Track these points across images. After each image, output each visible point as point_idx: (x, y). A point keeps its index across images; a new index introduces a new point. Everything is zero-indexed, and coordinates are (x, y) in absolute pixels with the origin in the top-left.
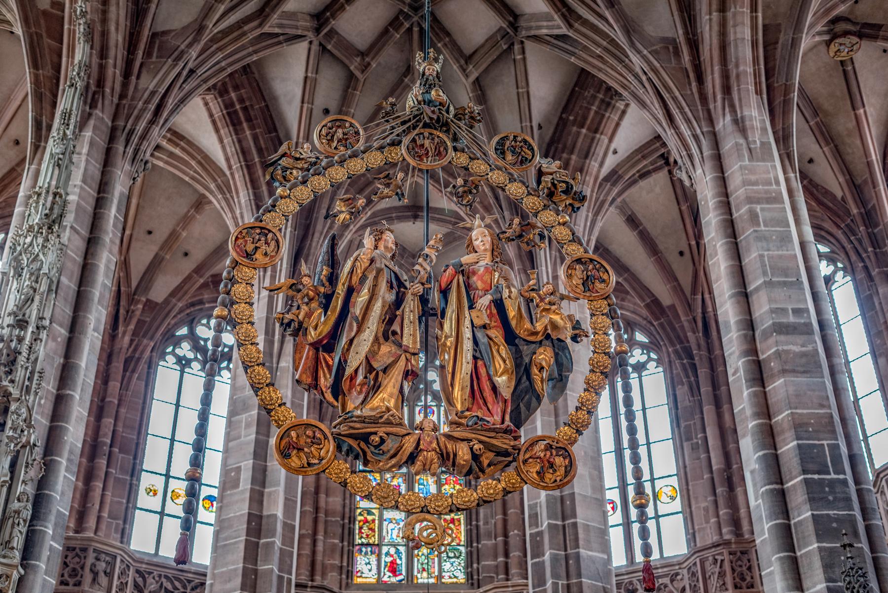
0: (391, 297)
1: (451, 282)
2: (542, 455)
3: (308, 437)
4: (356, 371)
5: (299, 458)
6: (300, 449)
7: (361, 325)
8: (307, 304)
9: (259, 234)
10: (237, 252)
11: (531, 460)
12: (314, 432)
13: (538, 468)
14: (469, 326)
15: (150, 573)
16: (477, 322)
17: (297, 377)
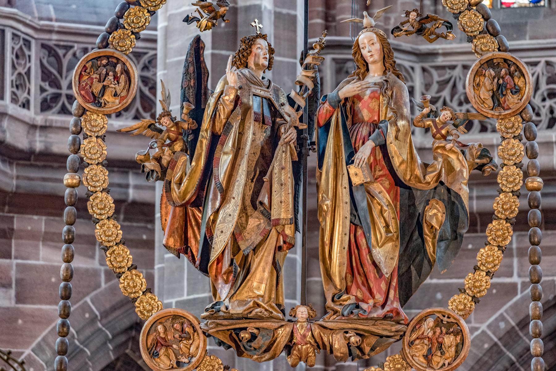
0: (262, 136)
1: (331, 116)
2: (430, 335)
3: (176, 330)
4: (223, 252)
5: (168, 356)
6: (168, 346)
7: (225, 193)
8: (169, 146)
9: (104, 66)
10: (83, 97)
11: (417, 342)
13: (425, 351)
14: (347, 186)
15: (68, 48)
16: (356, 181)
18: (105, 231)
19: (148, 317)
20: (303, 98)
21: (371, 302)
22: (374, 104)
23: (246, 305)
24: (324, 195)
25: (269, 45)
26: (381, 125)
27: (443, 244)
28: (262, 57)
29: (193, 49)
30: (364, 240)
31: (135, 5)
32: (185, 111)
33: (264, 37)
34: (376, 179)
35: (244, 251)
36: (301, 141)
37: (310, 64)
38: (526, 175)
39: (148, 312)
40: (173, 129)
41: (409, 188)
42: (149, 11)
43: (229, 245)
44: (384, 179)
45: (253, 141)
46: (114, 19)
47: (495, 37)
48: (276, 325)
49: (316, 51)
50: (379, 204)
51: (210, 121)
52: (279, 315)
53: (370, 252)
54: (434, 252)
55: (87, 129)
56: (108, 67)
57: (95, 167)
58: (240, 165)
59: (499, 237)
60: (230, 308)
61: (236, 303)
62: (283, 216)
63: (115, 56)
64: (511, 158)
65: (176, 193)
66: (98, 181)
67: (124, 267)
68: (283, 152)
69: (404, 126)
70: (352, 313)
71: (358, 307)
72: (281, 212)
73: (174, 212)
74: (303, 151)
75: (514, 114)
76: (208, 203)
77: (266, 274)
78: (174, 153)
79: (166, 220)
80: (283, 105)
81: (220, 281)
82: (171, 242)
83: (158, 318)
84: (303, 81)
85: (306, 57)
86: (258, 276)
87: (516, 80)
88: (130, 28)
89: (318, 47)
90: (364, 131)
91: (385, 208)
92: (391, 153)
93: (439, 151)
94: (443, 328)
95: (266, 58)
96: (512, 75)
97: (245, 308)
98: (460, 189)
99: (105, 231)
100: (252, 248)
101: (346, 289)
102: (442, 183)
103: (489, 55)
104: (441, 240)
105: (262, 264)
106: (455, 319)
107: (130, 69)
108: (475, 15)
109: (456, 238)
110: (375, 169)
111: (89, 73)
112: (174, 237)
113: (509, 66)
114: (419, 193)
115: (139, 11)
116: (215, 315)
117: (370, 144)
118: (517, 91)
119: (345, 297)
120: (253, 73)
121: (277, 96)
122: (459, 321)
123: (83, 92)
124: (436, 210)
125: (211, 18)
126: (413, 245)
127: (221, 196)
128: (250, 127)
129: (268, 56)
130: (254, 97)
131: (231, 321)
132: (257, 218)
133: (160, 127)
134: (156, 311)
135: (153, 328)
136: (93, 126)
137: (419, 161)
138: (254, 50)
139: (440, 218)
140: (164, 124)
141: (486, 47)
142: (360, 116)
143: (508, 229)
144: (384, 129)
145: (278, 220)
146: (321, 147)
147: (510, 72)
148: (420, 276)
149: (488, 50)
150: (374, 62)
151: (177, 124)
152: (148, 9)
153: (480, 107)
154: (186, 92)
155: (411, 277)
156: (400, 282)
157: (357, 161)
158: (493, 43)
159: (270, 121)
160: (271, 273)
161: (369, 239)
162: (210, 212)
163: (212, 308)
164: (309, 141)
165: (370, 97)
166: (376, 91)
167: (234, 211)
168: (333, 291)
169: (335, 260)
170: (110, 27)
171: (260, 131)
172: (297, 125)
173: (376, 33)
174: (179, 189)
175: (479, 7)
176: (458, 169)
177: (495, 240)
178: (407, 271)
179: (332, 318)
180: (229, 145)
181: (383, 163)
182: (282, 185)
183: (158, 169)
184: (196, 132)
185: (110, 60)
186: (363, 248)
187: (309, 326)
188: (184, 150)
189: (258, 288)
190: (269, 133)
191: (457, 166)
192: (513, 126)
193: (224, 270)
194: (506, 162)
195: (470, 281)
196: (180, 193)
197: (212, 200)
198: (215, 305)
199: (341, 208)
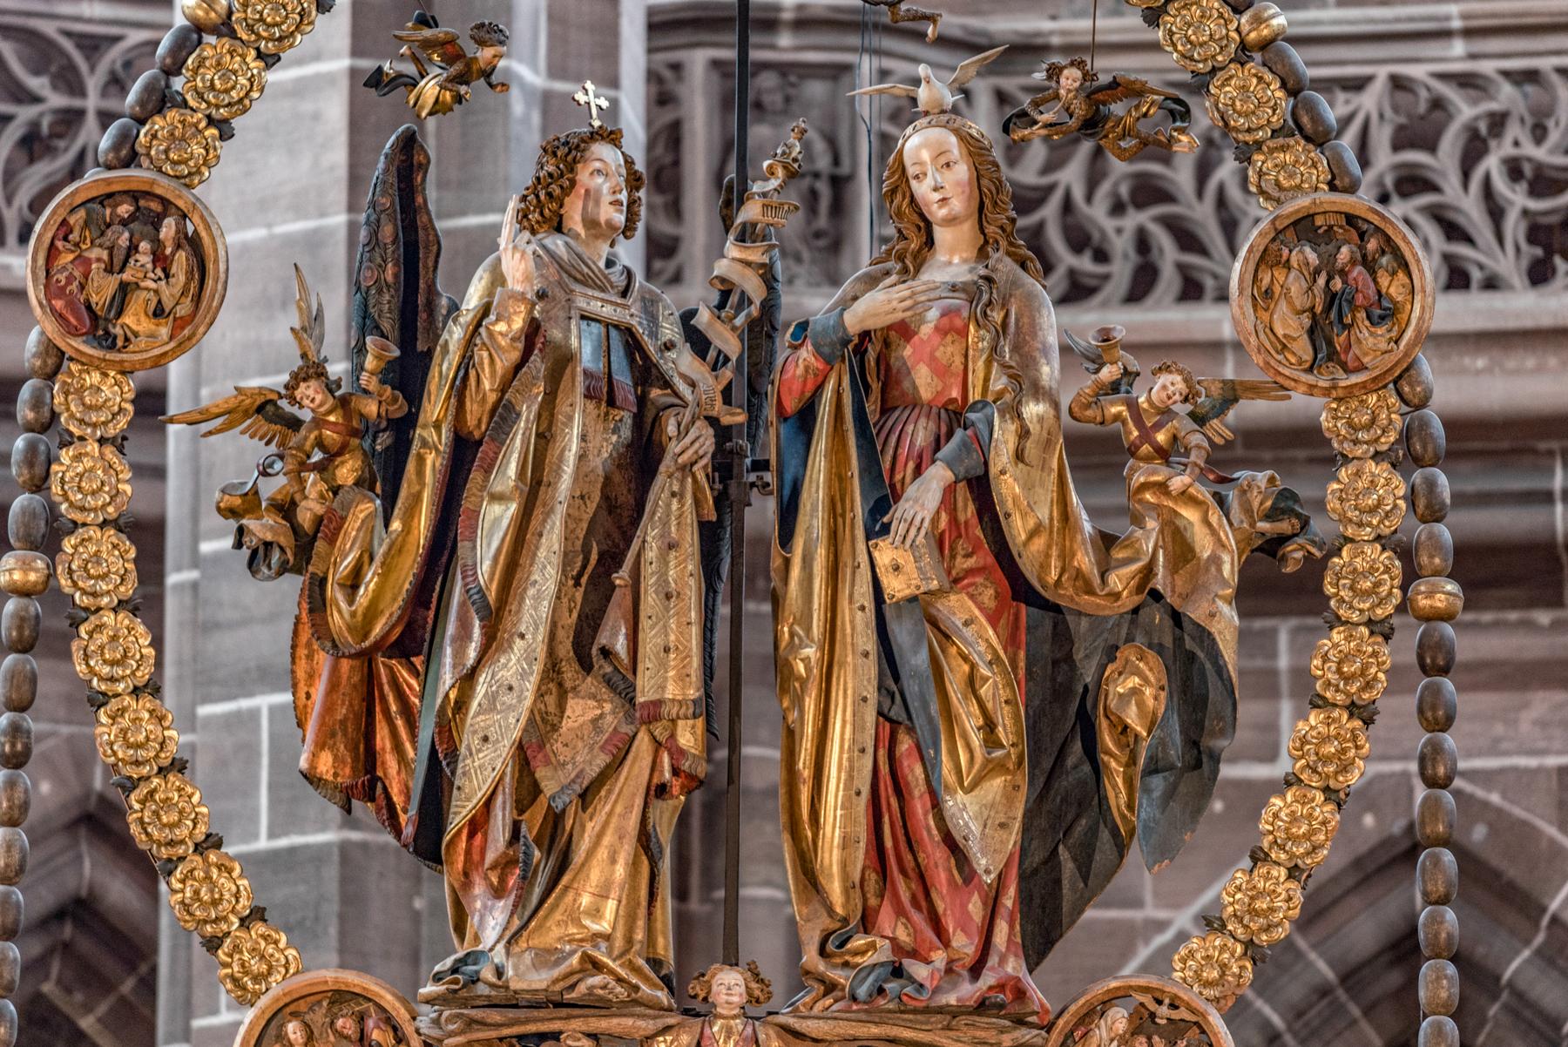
0: (608, 444)
1: (820, 388)
4: (489, 803)
7: (495, 620)
8: (321, 468)
9: (124, 223)
10: (60, 317)
12: (361, 1018)
16: (896, 587)
17: (303, 763)
18: (124, 731)
19: (257, 995)
20: (734, 329)
21: (939, 958)
22: (949, 352)
23: (557, 963)
24: (797, 628)
25: (629, 162)
26: (972, 416)
27: (1158, 783)
28: (607, 198)
29: (393, 169)
30: (918, 770)
31: (220, 35)
32: (370, 362)
33: (612, 137)
34: (956, 581)
35: (553, 797)
36: (724, 465)
37: (754, 225)
38: (1411, 575)
39: (256, 979)
40: (332, 418)
41: (1056, 609)
42: (260, 55)
43: (507, 779)
44: (979, 580)
45: (582, 457)
46: (154, 79)
47: (1320, 145)
48: (646, 1026)
49: (774, 183)
50: (965, 658)
51: (448, 398)
52: (659, 994)
53: (936, 805)
54: (1130, 807)
55: (72, 416)
56: (134, 226)
57: (93, 532)
58: (541, 535)
59: (1326, 760)
60: (510, 972)
61: (528, 958)
62: (672, 691)
63: (158, 191)
64: (1366, 518)
65: (340, 616)
66: (104, 577)
67: (182, 842)
68: (673, 494)
69: (1041, 419)
70: (881, 991)
71: (898, 972)
72: (666, 679)
73: (335, 670)
74: (733, 490)
75: (1377, 384)
76: (441, 647)
77: (620, 871)
78: (336, 490)
79: (308, 696)
80: (669, 346)
81: (479, 889)
82: (325, 764)
83: (287, 1000)
84: (735, 278)
85: (741, 202)
86: (595, 875)
87: (1384, 281)
88: (204, 105)
89: (780, 172)
90: (920, 433)
91: (984, 671)
92: (1003, 503)
93: (1148, 496)
94: (1156, 1039)
95: (617, 203)
96: (1370, 265)
97: (556, 972)
98: (1212, 615)
99: (124, 731)
100: (578, 789)
101: (864, 918)
102: (1156, 595)
103: (1302, 203)
104: (1153, 768)
105: (606, 840)
106: (1193, 1011)
107: (203, 234)
108: (1260, 79)
109: (1198, 765)
110: (952, 549)
111: (77, 245)
112: (331, 748)
113: (1362, 235)
114: (1084, 623)
115: (231, 53)
116: (463, 993)
117: (938, 476)
118: (1385, 313)
119: (859, 941)
120: (580, 249)
121: (653, 319)
122: (1203, 1015)
123: (59, 304)
124: (1137, 680)
125: (450, 80)
126: (1065, 783)
127: (482, 627)
128: (571, 418)
129: (623, 197)
130: (584, 324)
131: (512, 1014)
132: (593, 697)
133: (295, 410)
134: (279, 978)
135: (272, 1031)
136: (90, 408)
137: (1087, 527)
138: (583, 176)
139: (1150, 703)
140: (306, 402)
141: (1291, 176)
142: (906, 385)
143: (1355, 738)
144: (982, 427)
145: (658, 703)
146: (788, 478)
147: (1364, 256)
148: (1085, 879)
149: (1299, 187)
150: (951, 221)
151: (344, 403)
152: (258, 49)
153: (1272, 362)
154: (372, 302)
155: (1058, 882)
156: (1025, 898)
157: (898, 528)
158: (1314, 165)
159: (632, 398)
160: (634, 865)
161: (933, 766)
162: (447, 678)
163: (454, 970)
164: (748, 461)
165: (937, 328)
166: (957, 311)
167: (524, 675)
168: (825, 922)
169: (828, 829)
170: (142, 102)
171: (600, 427)
172: (714, 413)
173: (956, 132)
174: (351, 602)
175: (1270, 55)
176: (1205, 555)
177: (1315, 771)
178: (1045, 862)
179: (819, 1006)
180: (510, 470)
181: (979, 532)
182: (668, 596)
183: (286, 540)
184: (403, 428)
185: (142, 203)
186: (916, 793)
187: (749, 1030)
188: (364, 483)
189: (596, 913)
190: (626, 432)
191: (1203, 544)
192: (1373, 421)
193: (490, 857)
194: (1350, 532)
195: (1238, 896)
196: (353, 614)
197: (454, 640)
198: (463, 961)
199: (850, 669)
